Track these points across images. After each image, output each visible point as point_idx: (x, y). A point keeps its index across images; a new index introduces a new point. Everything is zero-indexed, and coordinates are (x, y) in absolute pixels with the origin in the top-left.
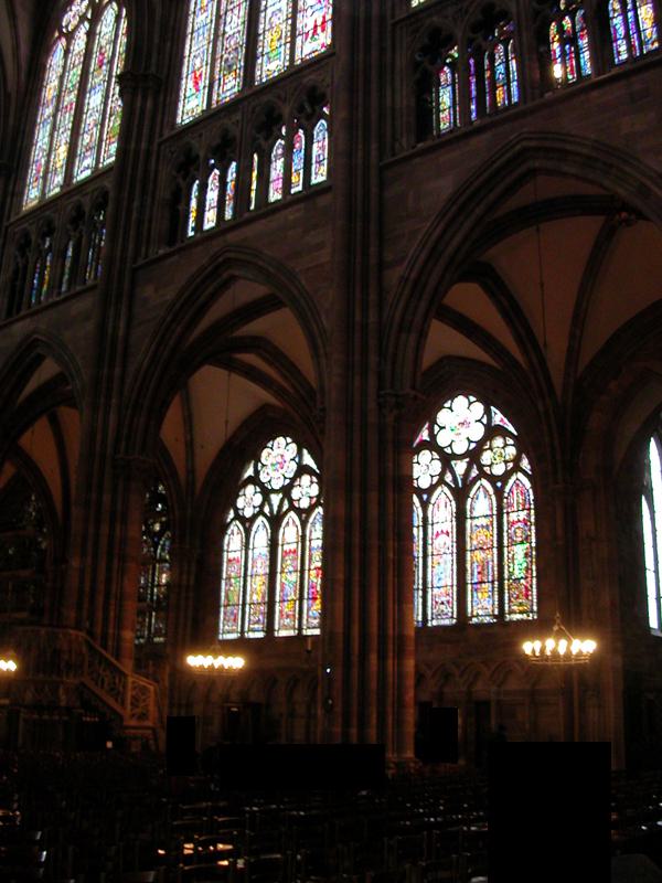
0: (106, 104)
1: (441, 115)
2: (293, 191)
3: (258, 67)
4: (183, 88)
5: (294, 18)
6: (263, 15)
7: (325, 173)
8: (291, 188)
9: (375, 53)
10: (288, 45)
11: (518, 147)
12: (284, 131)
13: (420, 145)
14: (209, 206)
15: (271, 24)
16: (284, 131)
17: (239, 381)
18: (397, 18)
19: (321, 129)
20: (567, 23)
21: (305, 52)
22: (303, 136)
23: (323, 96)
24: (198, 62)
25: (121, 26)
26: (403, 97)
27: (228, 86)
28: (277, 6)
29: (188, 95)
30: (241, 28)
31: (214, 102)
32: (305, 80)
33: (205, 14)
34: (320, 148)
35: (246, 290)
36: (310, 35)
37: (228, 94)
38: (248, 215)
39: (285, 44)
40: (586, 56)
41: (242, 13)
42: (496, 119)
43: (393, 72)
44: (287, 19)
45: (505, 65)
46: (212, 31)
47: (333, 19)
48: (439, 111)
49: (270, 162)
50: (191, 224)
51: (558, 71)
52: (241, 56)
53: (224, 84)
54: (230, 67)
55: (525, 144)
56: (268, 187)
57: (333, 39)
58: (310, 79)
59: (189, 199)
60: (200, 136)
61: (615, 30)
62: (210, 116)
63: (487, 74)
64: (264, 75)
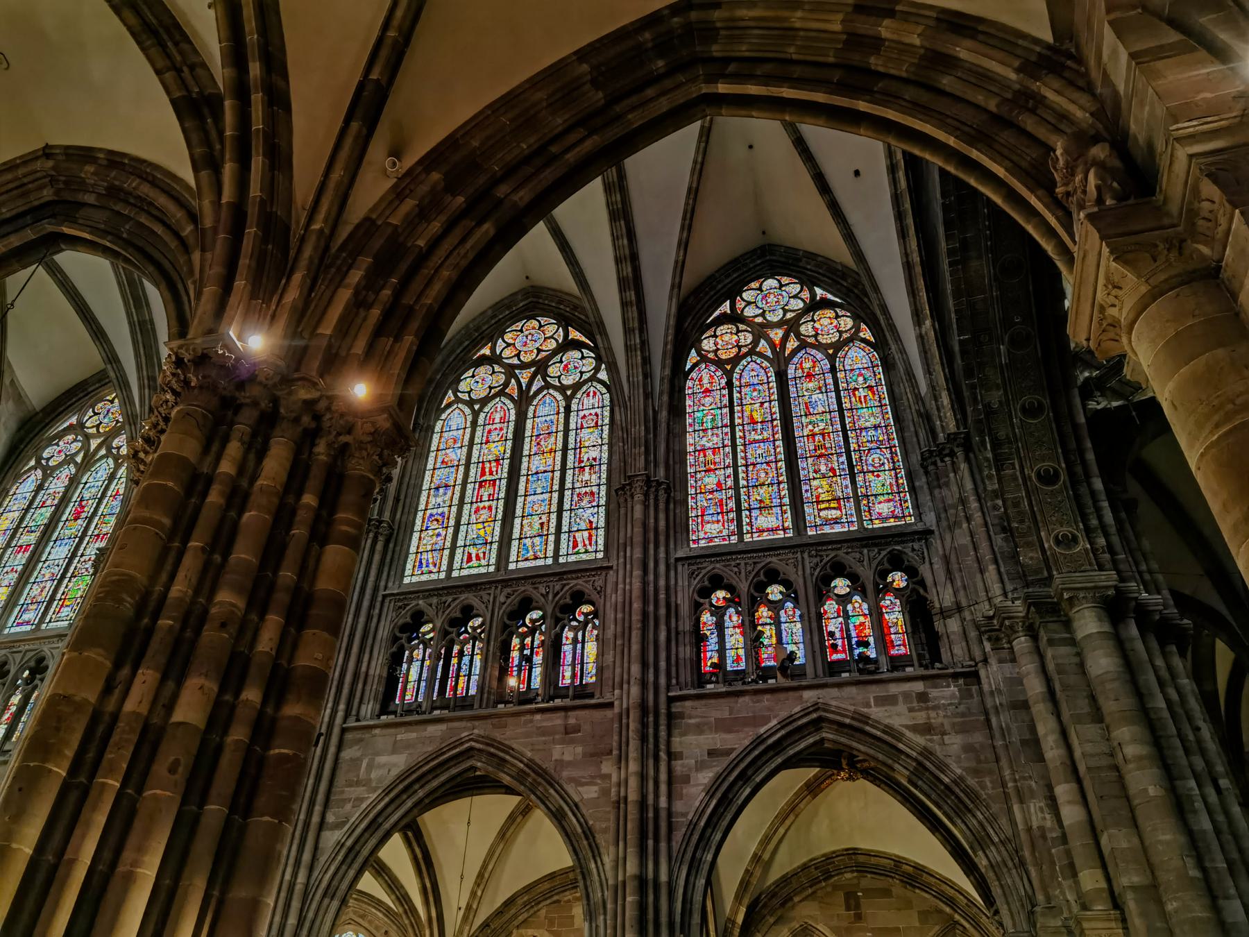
11: (467, 745)
18: (387, 592)
26: (377, 666)
55: (473, 744)
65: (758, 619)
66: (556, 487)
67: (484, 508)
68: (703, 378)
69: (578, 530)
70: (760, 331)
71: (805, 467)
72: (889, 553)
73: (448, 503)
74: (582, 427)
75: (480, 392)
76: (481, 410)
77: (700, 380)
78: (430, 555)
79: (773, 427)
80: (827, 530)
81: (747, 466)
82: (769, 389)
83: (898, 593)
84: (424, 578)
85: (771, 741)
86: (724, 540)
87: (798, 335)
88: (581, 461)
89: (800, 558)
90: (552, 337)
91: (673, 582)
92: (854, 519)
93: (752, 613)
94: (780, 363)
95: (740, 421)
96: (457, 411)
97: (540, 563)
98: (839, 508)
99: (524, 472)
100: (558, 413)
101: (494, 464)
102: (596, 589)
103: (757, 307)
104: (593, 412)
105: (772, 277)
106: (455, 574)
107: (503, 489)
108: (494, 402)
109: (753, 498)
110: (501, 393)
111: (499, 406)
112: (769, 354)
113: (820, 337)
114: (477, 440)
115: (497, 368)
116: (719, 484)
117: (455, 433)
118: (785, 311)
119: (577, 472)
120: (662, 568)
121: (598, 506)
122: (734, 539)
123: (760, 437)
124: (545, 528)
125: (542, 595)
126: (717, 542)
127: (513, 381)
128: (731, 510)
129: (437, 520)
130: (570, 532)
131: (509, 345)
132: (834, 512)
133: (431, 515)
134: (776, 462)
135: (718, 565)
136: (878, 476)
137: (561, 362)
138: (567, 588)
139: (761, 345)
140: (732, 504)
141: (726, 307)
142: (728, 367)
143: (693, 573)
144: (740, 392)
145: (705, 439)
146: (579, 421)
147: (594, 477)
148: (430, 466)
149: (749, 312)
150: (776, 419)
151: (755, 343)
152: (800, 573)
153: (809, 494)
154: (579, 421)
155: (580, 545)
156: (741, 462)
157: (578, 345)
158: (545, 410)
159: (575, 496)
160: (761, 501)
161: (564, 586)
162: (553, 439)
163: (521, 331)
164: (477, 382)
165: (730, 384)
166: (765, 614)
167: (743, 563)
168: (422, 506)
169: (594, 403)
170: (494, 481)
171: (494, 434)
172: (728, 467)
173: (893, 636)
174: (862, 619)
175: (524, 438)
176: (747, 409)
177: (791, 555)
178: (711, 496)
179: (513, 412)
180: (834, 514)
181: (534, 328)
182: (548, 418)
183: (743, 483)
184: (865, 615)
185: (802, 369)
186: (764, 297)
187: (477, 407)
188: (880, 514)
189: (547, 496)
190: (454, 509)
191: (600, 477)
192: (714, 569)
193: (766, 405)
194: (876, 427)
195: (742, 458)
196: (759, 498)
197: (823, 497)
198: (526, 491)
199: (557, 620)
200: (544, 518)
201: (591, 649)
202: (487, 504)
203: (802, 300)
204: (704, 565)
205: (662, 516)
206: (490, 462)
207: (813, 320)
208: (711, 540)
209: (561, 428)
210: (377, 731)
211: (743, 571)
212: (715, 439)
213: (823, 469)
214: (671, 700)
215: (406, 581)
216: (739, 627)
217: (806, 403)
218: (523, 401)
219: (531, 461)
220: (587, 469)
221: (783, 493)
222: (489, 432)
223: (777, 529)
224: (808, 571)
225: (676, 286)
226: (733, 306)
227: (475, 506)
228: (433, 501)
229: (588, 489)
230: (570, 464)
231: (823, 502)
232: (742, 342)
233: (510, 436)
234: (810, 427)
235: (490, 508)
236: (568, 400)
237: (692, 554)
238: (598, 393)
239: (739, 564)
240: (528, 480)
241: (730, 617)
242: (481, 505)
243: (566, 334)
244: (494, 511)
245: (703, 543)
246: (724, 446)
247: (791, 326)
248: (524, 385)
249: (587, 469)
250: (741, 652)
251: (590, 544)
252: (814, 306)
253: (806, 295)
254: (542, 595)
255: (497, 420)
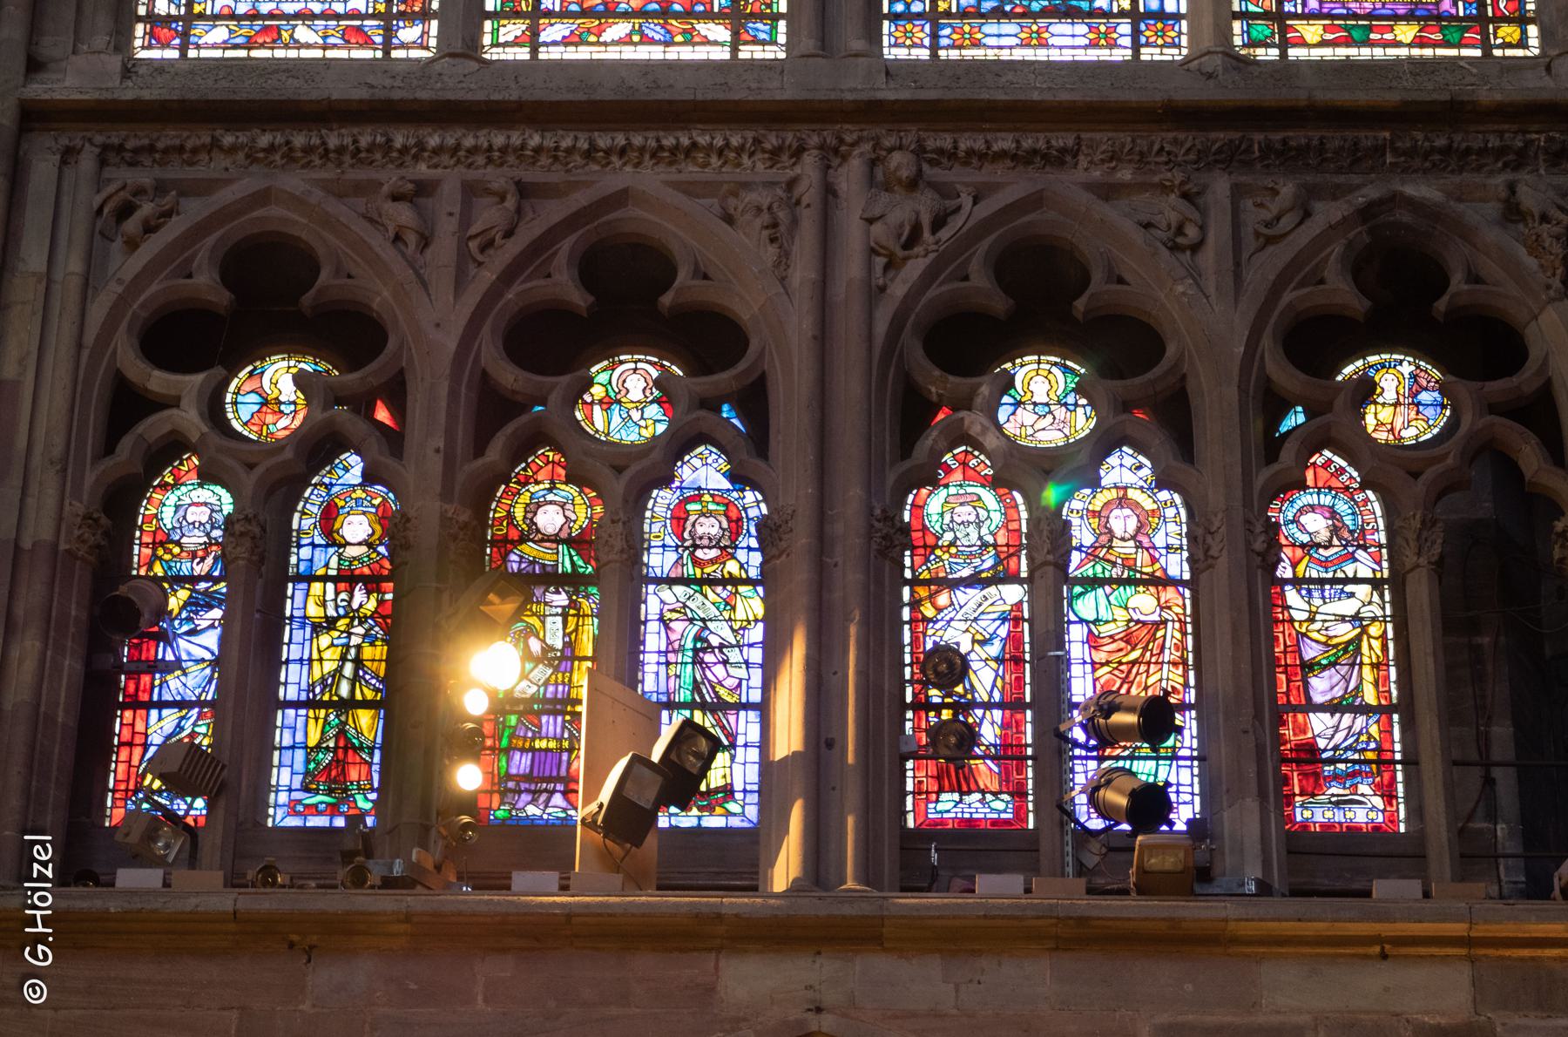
65: (505, 545)
72: (1366, 213)
89: (809, 189)
135: (293, 181)
143: (125, 211)
152: (802, 272)
167: (451, 179)
173: (1319, 723)
177: (758, 168)
192: (262, 197)
211: (447, 228)
216: (372, 583)
224: (851, 267)
239: (423, 189)
241: (329, 516)
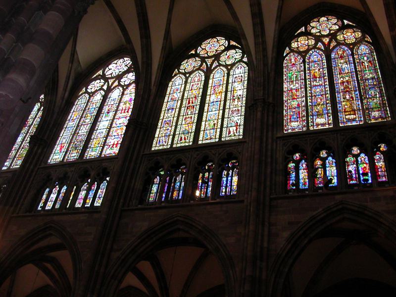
0: (22, 143)
1: (151, 195)
2: (86, 206)
3: (87, 152)
4: (55, 149)
5: (107, 138)
6: (95, 132)
7: (100, 203)
8: (85, 204)
9: (132, 164)
10: (101, 148)
11: (175, 219)
12: (89, 181)
13: (139, 206)
14: (51, 199)
15: (97, 136)
16: (89, 181)
17: (41, 273)
18: (145, 153)
19: (104, 185)
20: (207, 175)
21: (107, 153)
22: (96, 185)
23: (109, 173)
24: (64, 140)
25: (39, 114)
26: (139, 185)
27: (73, 155)
28: (102, 131)
29: (56, 152)
30: (85, 133)
31: (65, 159)
32: (104, 164)
33: (73, 123)
34: (102, 192)
35: (54, 240)
36: (111, 147)
37: (72, 158)
38: (66, 209)
39: (100, 147)
40: (210, 189)
41: (87, 128)
42: (170, 201)
43: (137, 173)
44: (104, 137)
45: (180, 182)
46: (74, 131)
47: (121, 144)
48: (151, 193)
49: (80, 191)
50: (41, 204)
51: (198, 193)
52: (82, 145)
53: (72, 153)
54: (76, 147)
55: (179, 218)
56: (76, 201)
57: (119, 151)
58: (105, 164)
59: (43, 194)
60: (56, 171)
61: (223, 182)
62: (62, 164)
63: (172, 185)
64: (88, 156)
65: (315, 166)
66: (221, 108)
67: (189, 117)
68: (291, 61)
69: (231, 126)
70: (318, 38)
71: (339, 97)
73: (173, 116)
74: (235, 82)
75: (189, 69)
76: (189, 76)
77: (291, 60)
78: (164, 138)
79: (324, 79)
80: (349, 124)
81: (312, 96)
82: (323, 63)
83: (382, 152)
84: (161, 148)
85: (319, 218)
86: (301, 129)
87: (336, 40)
88: (233, 96)
90: (223, 45)
91: (275, 147)
92: (362, 119)
93: (313, 161)
94: (328, 52)
95: (309, 77)
96: (179, 77)
97: (213, 141)
98: (355, 114)
99: (207, 102)
100: (224, 76)
101: (194, 99)
102: (238, 152)
103: (317, 29)
104: (240, 75)
105: (324, 17)
106: (174, 146)
107: (198, 109)
108: (195, 73)
109: (314, 111)
110: (199, 69)
111: (197, 75)
112: (323, 48)
113: (346, 41)
114: (187, 89)
115: (197, 58)
116: (298, 105)
117: (177, 87)
118: (330, 30)
119: (231, 101)
120: (270, 140)
121: (241, 116)
122: (305, 129)
123: (318, 84)
124: (216, 125)
125: (213, 154)
126: (297, 130)
127: (204, 64)
128: (304, 116)
129: (168, 123)
130: (227, 127)
131: (203, 49)
132: (352, 116)
133: (165, 121)
134: (326, 95)
136: (374, 100)
137: (226, 55)
138: (225, 151)
139: (319, 45)
140: (304, 113)
141: (303, 29)
142: (304, 54)
144: (309, 65)
145: (292, 85)
146: (234, 79)
147: (239, 103)
148: (166, 101)
149: (313, 31)
150: (326, 76)
151: (316, 44)
153: (341, 109)
154: (234, 79)
155: (232, 133)
156: (309, 95)
157: (234, 47)
158: (218, 75)
159: (230, 112)
160: (318, 112)
161: (224, 150)
162: (221, 87)
163: (209, 43)
164: (188, 65)
165: (304, 62)
166: (319, 163)
168: (161, 118)
169: (241, 71)
170: (194, 106)
171: (195, 86)
172: (303, 97)
174: (365, 165)
175: (208, 87)
176: (312, 72)
178: (294, 110)
179: (203, 77)
180: (352, 117)
181: (215, 42)
182: (219, 79)
183: (309, 104)
184: (366, 164)
185: (338, 54)
186: (320, 25)
187: (187, 75)
188: (374, 117)
189: (217, 112)
190: (175, 119)
191: (242, 103)
193: (321, 70)
194: (372, 78)
195: (309, 93)
196: (317, 110)
197: (347, 110)
198: (208, 110)
199: (220, 166)
200: (216, 122)
201: (235, 179)
202: (190, 116)
203: (338, 25)
204: (290, 140)
205: (270, 118)
206: (192, 98)
207: (343, 34)
208: (293, 129)
209: (225, 82)
210: (137, 212)
212: (297, 85)
213: (348, 97)
214: (271, 199)
215: (153, 149)
217: (340, 69)
218: (208, 73)
219: (211, 97)
220: (236, 100)
221: (328, 108)
222: (193, 85)
223: (326, 124)
225: (279, 17)
226: (306, 29)
227: (184, 117)
228: (166, 115)
229: (236, 109)
230: (228, 98)
231: (347, 112)
232: (310, 43)
233: (202, 87)
234: (342, 79)
235: (191, 117)
236: (229, 71)
237: (284, 135)
238: (243, 67)
240: (209, 105)
241: (302, 165)
242: (188, 116)
243: (229, 43)
244: (193, 119)
245: (290, 131)
246: (301, 88)
247: (333, 36)
248: (209, 65)
249: (236, 100)
250: (307, 180)
251: (237, 132)
252: (343, 28)
253: (340, 23)
254: (213, 154)
255: (196, 80)
